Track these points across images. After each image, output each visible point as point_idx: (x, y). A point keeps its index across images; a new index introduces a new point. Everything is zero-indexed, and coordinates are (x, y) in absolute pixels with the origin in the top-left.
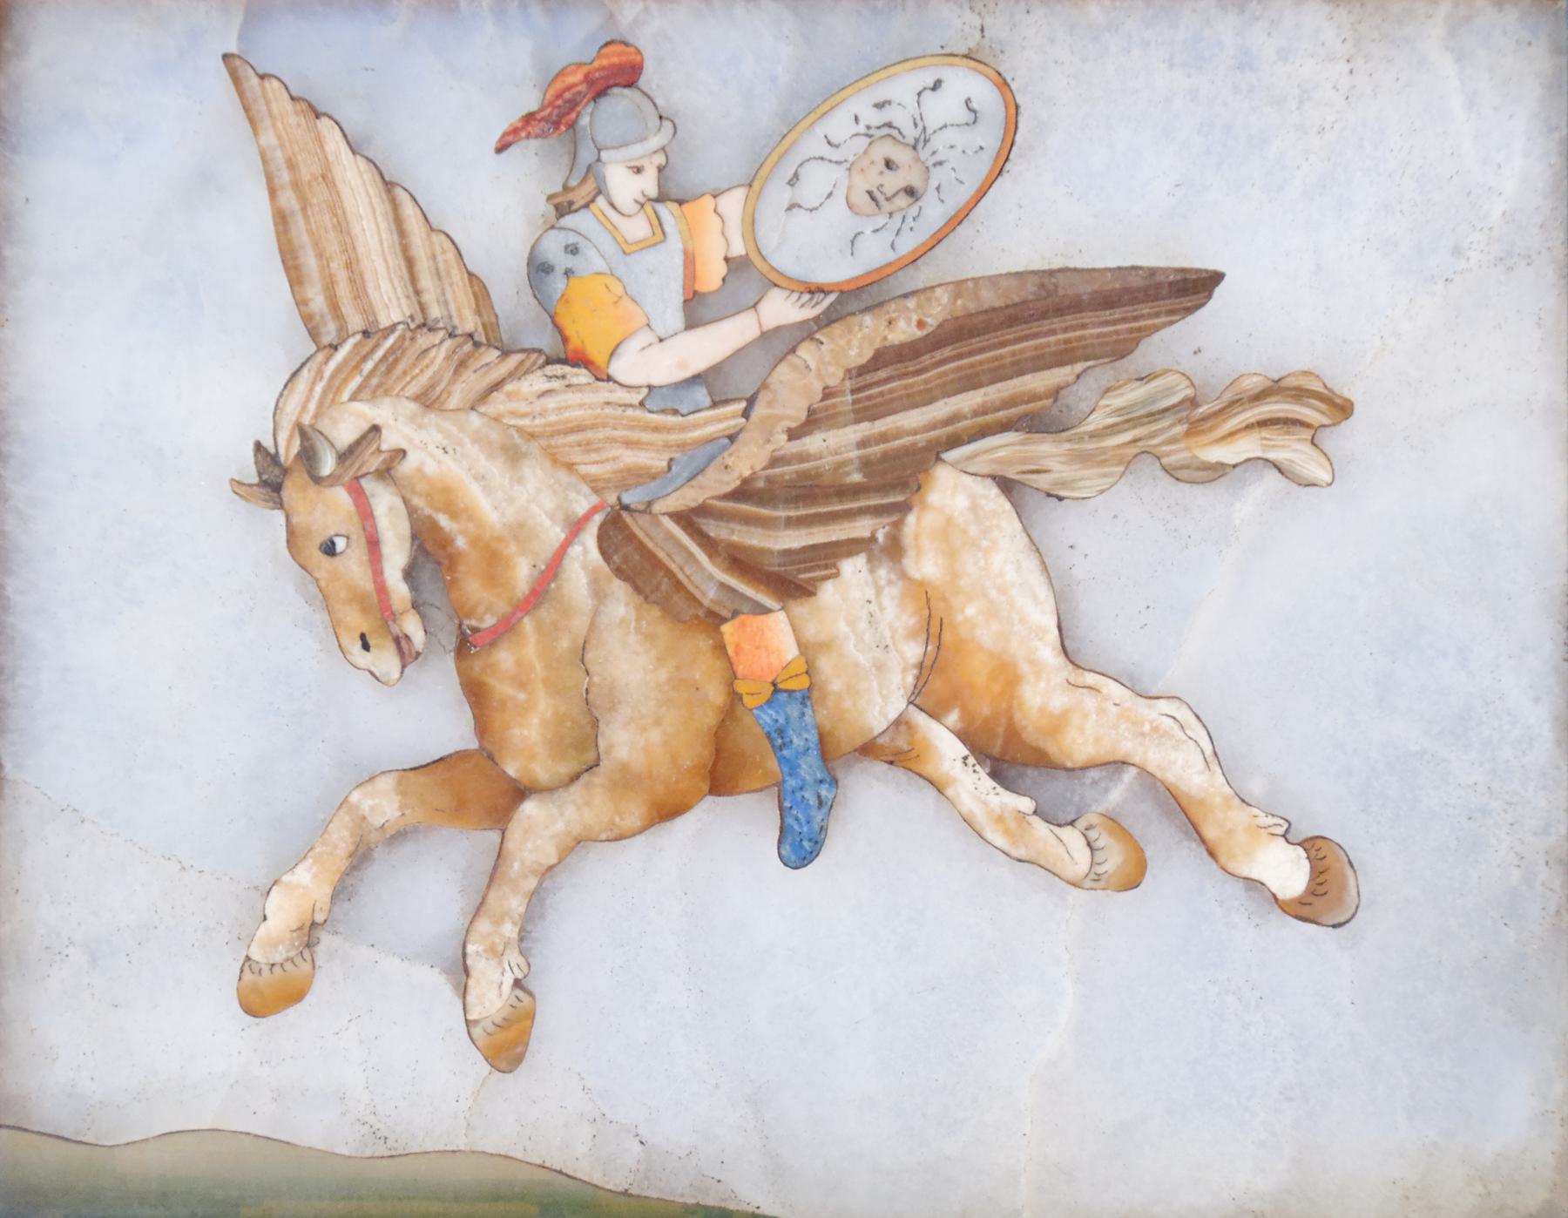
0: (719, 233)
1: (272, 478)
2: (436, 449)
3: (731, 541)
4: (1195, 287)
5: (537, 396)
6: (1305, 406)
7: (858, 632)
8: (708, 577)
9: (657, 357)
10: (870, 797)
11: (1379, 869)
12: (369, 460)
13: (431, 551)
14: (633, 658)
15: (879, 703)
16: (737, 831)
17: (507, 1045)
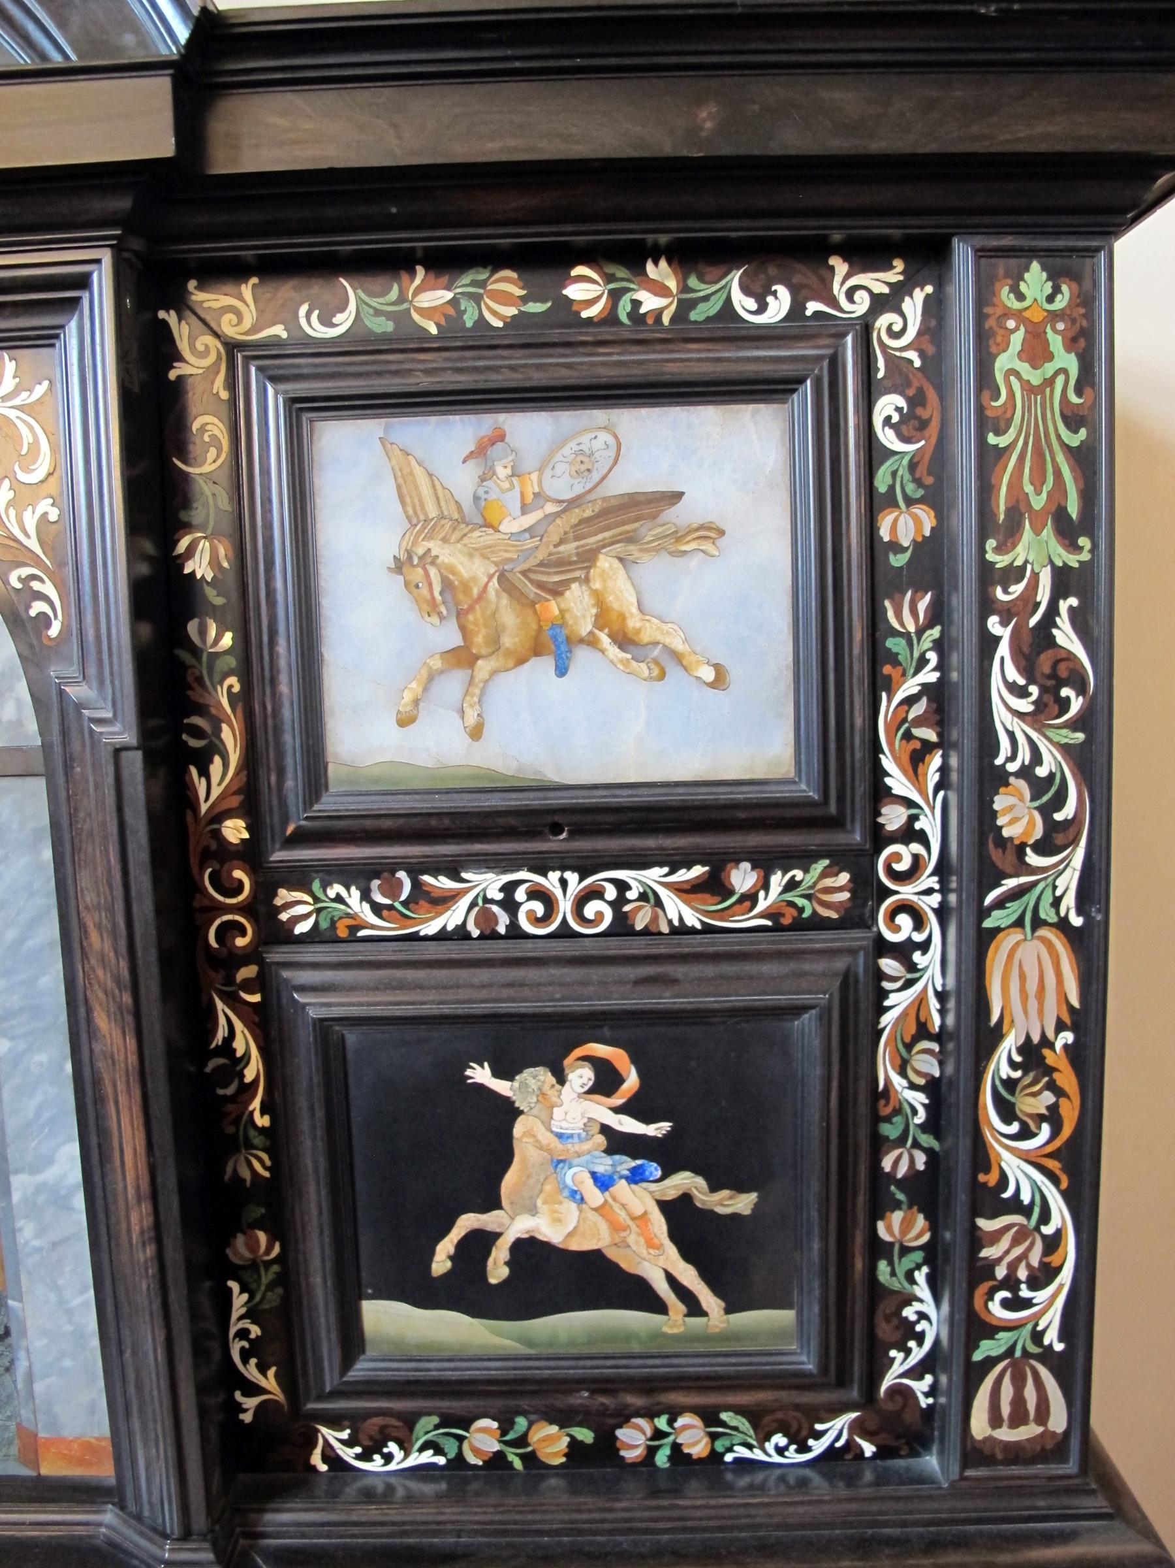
0: (532, 487)
1: (399, 566)
2: (446, 554)
3: (540, 578)
4: (677, 496)
5: (480, 538)
6: (711, 532)
7: (577, 604)
8: (532, 590)
9: (511, 526)
10: (582, 657)
11: (735, 673)
12: (427, 559)
13: (447, 585)
14: (509, 617)
15: (585, 627)
16: (543, 666)
17: (476, 733)
